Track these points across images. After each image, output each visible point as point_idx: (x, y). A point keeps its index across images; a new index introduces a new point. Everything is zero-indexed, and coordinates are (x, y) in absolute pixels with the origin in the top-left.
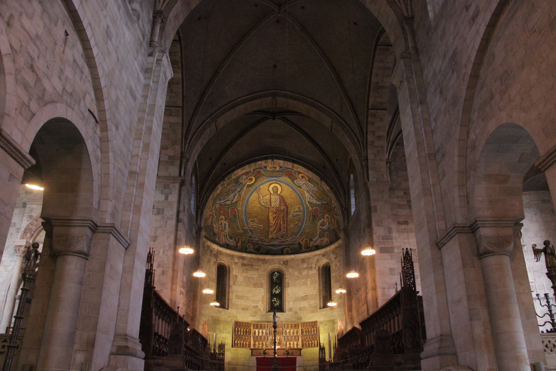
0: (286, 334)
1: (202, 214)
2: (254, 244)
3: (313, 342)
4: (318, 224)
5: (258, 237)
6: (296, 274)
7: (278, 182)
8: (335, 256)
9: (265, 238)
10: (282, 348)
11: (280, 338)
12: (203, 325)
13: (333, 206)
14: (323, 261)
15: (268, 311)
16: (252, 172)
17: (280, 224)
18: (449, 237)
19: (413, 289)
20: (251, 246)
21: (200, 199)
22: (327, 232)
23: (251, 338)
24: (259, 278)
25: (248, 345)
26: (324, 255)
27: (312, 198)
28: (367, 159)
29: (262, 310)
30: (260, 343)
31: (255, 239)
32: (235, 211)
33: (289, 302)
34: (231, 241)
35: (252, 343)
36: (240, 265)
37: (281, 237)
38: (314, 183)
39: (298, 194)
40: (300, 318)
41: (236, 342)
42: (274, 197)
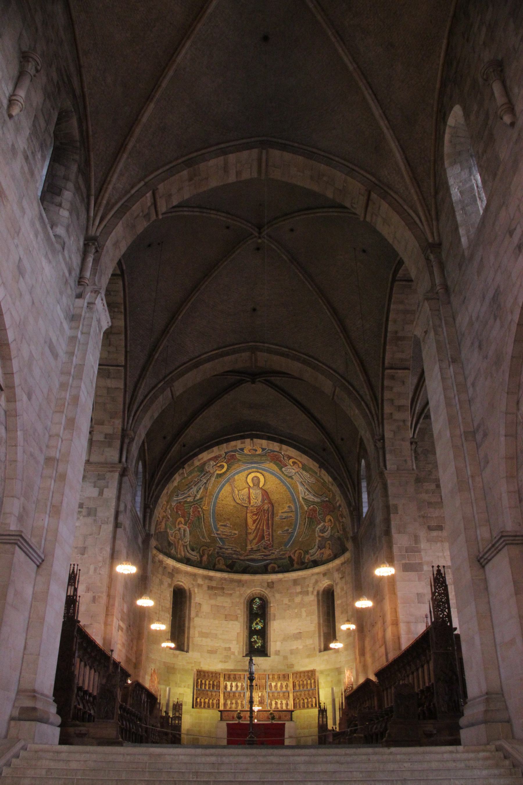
0: (271, 689)
1: (151, 517)
2: (225, 558)
3: (310, 700)
4: (317, 529)
5: (232, 549)
6: (286, 601)
7: (260, 471)
8: (340, 576)
9: (242, 550)
10: (264, 710)
11: (262, 694)
12: (152, 675)
13: (338, 504)
14: (323, 582)
15: (244, 655)
16: (223, 456)
17: (264, 530)
18: (495, 550)
19: (449, 624)
20: (222, 562)
21: (149, 494)
22: (329, 542)
23: (221, 694)
24: (232, 606)
25: (215, 705)
26: (325, 574)
27: (307, 493)
28: (383, 438)
29: (236, 654)
30: (234, 701)
31: (227, 551)
32: (199, 511)
33: (276, 642)
34: (194, 553)
35: (222, 701)
36: (205, 588)
37: (265, 548)
38: (310, 472)
39: (288, 488)
40: (292, 666)
41: (198, 700)
42: (254, 492)
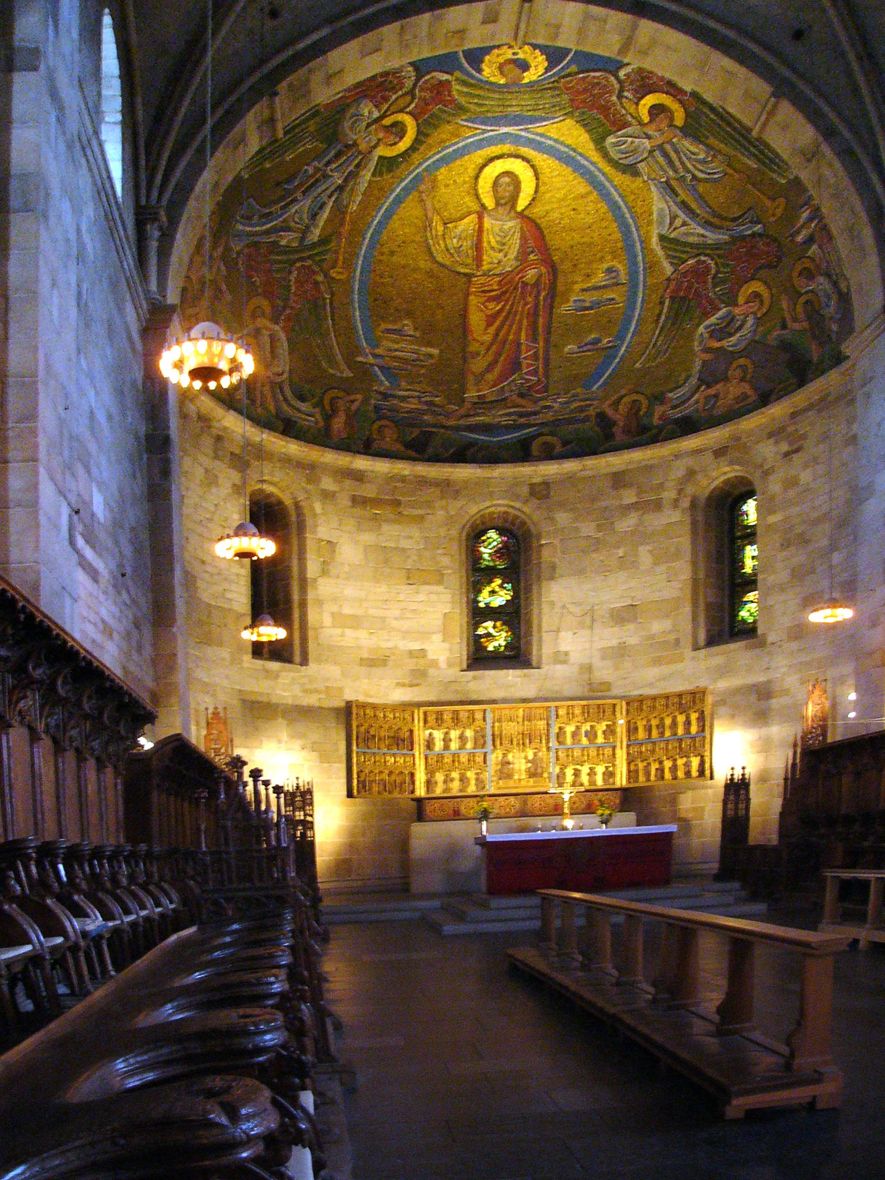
16: (409, 84)
